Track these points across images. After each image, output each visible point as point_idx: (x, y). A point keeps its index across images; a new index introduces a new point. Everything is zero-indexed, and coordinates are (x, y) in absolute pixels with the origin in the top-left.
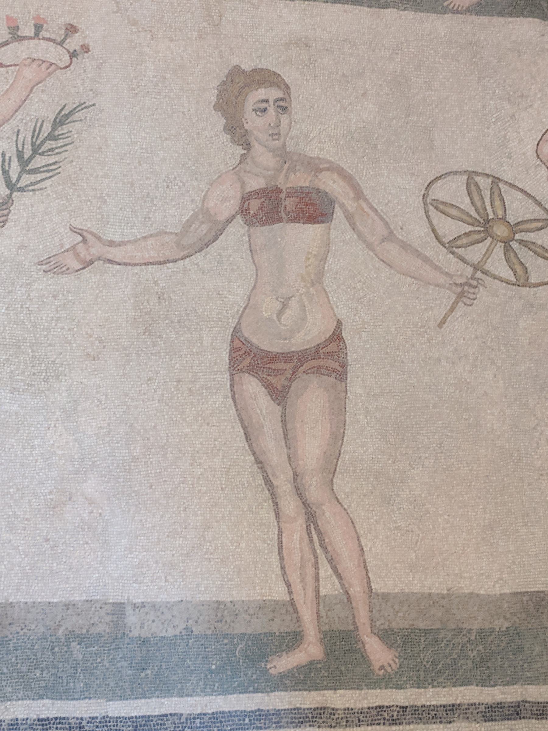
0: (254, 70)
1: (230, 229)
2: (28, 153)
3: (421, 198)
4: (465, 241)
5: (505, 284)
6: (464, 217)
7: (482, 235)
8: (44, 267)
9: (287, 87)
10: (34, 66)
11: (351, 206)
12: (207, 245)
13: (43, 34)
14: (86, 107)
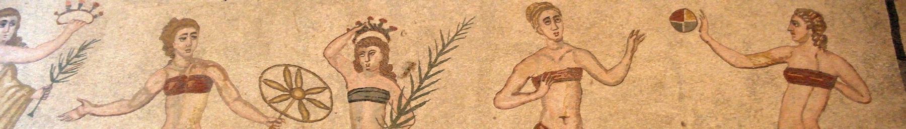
0: (183, 20)
1: (157, 97)
2: (64, 64)
3: (258, 79)
4: (278, 100)
5: (296, 121)
6: (280, 87)
7: (288, 96)
8: (61, 118)
9: (198, 27)
10: (75, 23)
11: (221, 83)
12: (144, 105)
13: (83, 8)
14: (96, 41)
